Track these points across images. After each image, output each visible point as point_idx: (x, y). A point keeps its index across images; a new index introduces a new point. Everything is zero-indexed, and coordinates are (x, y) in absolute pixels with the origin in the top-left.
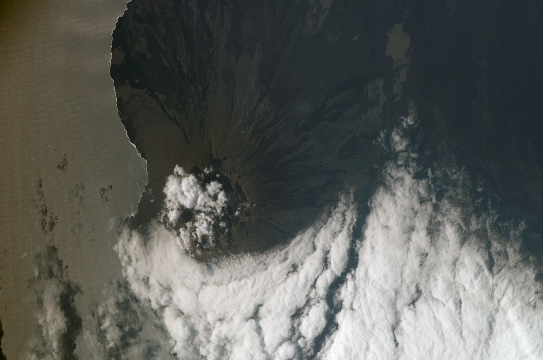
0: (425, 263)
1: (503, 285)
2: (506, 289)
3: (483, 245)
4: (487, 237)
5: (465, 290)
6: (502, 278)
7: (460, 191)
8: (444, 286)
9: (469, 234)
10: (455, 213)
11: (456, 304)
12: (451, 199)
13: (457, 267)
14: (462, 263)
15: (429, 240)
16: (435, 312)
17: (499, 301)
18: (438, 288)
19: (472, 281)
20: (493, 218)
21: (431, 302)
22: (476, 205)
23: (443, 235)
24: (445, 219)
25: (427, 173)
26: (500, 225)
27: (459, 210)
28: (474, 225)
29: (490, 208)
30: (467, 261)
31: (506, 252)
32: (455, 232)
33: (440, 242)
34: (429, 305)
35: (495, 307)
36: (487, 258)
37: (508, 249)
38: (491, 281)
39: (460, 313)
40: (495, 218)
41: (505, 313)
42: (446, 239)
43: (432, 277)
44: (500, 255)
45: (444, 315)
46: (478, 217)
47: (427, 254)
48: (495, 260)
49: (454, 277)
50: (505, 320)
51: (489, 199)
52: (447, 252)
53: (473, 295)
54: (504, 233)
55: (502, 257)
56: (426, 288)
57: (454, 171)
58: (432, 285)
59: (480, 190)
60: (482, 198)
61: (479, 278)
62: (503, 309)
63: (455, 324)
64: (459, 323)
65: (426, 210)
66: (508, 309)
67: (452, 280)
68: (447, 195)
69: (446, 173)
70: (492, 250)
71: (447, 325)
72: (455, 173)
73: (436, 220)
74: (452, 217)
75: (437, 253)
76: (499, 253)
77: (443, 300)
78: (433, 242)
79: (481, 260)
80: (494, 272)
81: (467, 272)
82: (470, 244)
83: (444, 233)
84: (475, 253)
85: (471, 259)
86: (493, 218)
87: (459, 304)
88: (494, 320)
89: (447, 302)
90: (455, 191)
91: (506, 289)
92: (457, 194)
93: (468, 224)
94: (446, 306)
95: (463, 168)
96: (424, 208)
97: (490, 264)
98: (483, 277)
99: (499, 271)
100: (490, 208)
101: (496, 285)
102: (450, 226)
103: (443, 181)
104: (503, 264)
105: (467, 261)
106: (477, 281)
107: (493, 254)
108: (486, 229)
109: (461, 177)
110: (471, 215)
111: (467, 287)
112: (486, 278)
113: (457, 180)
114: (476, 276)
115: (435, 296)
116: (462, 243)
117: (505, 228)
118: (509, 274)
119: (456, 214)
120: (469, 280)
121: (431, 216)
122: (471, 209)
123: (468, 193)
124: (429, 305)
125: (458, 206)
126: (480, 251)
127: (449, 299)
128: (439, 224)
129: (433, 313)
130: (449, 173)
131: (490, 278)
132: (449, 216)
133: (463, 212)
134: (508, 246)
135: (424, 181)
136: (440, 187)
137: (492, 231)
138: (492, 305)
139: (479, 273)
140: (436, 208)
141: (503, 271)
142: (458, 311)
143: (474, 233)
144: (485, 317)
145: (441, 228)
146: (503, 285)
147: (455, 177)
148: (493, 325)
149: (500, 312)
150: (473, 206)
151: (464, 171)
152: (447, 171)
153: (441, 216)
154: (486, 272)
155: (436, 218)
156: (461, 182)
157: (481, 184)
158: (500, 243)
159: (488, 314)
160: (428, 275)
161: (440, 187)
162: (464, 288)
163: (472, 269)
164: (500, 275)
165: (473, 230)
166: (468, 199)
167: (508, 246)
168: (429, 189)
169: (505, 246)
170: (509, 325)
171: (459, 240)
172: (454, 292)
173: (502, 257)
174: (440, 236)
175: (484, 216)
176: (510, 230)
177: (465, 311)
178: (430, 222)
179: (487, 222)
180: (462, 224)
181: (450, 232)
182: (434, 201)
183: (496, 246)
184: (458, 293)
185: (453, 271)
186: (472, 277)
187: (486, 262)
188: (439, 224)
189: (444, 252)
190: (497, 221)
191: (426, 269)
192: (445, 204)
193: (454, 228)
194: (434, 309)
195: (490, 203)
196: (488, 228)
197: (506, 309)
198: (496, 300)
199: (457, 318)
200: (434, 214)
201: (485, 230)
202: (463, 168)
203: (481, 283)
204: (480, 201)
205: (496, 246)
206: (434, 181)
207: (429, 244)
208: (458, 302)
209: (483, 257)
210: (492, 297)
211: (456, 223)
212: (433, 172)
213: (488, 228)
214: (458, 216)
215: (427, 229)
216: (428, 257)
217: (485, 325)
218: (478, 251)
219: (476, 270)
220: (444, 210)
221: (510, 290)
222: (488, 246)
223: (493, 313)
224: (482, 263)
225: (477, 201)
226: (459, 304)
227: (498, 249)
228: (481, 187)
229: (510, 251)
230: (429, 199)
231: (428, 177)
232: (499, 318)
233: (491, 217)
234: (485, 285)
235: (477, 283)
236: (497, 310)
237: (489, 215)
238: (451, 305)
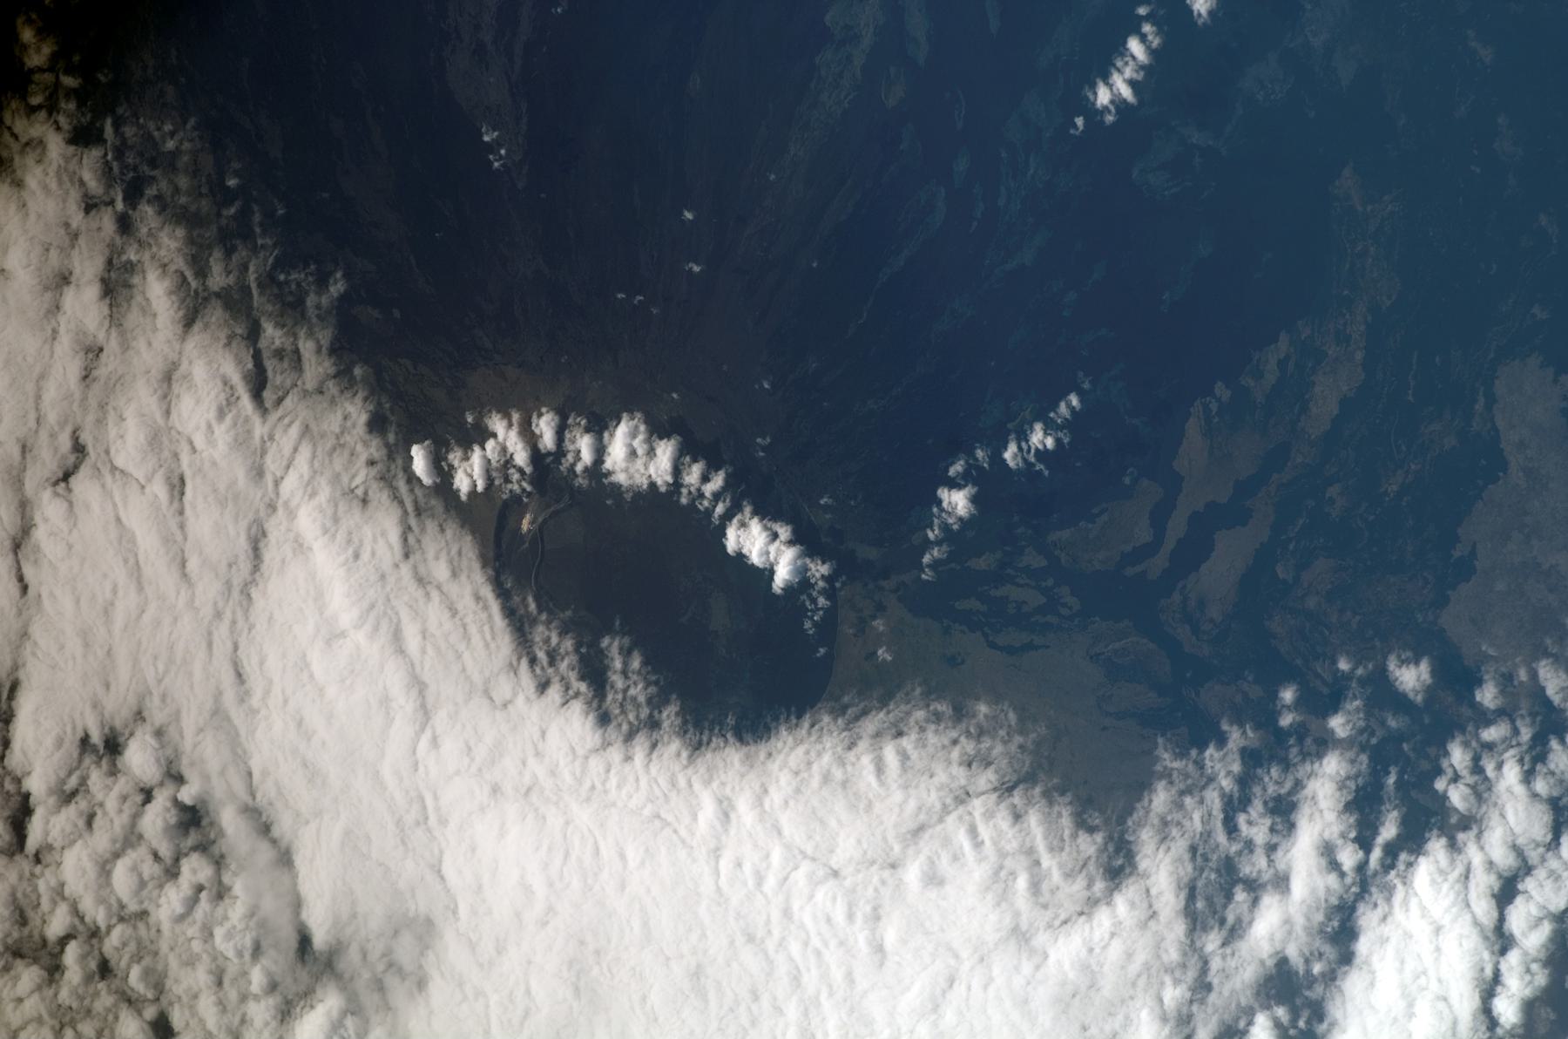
0: (95, 373)
1: (287, 439)
2: (296, 450)
3: (239, 331)
4: (250, 307)
5: (194, 450)
6: (286, 421)
7: (183, 182)
8: (142, 437)
9: (206, 299)
10: (170, 243)
11: (172, 487)
12: (161, 203)
13: (176, 387)
14: (187, 377)
15: (106, 311)
16: (120, 505)
17: (277, 483)
18: (127, 443)
19: (209, 426)
20: (266, 259)
21: (108, 478)
22: (224, 222)
23: (139, 298)
24: (147, 256)
25: (102, 130)
26: (282, 277)
27: (180, 232)
28: (218, 278)
29: (258, 230)
30: (199, 371)
31: (297, 351)
32: (171, 293)
33: (133, 318)
34: (103, 486)
35: (267, 500)
36: (250, 366)
37: (300, 345)
38: (259, 429)
39: (181, 512)
40: (271, 260)
41: (292, 515)
42: (147, 310)
43: (112, 412)
44: (281, 359)
45: (140, 513)
46: (229, 252)
47: (101, 350)
48: (270, 374)
49: (168, 413)
50: (292, 535)
51: (256, 208)
52: (150, 344)
53: (214, 463)
54: (290, 299)
55: (286, 364)
56: (96, 439)
57: (168, 127)
58: (113, 432)
59: (232, 182)
60: (237, 205)
61: (229, 419)
62: (286, 503)
63: (167, 540)
64: (179, 538)
65: (99, 229)
66: (299, 505)
67: (160, 421)
68: (151, 191)
69: (150, 137)
70: (262, 344)
71: (148, 542)
72: (172, 134)
73: (124, 258)
74: (163, 253)
75: (125, 347)
76: (279, 354)
77: (140, 474)
78: (116, 316)
79: (232, 368)
80: (268, 404)
81: (198, 402)
82: (206, 326)
83: (144, 293)
84: (220, 351)
85: (210, 367)
86: (266, 259)
87: (178, 486)
88: (264, 534)
89: (149, 480)
90: (171, 181)
91: (296, 450)
92: (177, 190)
93: (202, 273)
94: (147, 490)
95: (192, 122)
96: (94, 225)
97: (258, 383)
98: (237, 416)
99: (280, 401)
100: (258, 230)
101: (271, 438)
102: (158, 279)
103: (141, 154)
104: (288, 383)
105: (199, 371)
106: (224, 427)
107: (265, 354)
108: (249, 287)
109: (187, 146)
110: (210, 247)
111: (199, 441)
112: (247, 420)
113: (176, 154)
114: (221, 414)
115: (120, 461)
116: (189, 322)
117: (293, 287)
118: (304, 413)
119: (174, 245)
120: (203, 426)
121: (111, 245)
122: (211, 232)
123: (204, 190)
124: (103, 486)
125: (178, 223)
126: (234, 344)
127: (154, 472)
128: (130, 268)
129: (115, 505)
130: (156, 134)
131: (256, 420)
132: (154, 249)
133: (190, 241)
134: (302, 334)
135: (96, 153)
136: (135, 169)
137: (261, 294)
138: (259, 495)
139: (229, 404)
140: (125, 225)
141: (288, 402)
142: (176, 504)
143: (218, 295)
144: (244, 524)
145: (136, 280)
146: (287, 439)
147: (171, 145)
148: (261, 545)
149: (280, 511)
150: (213, 229)
151: (194, 128)
152: (152, 125)
153: (136, 246)
154: (246, 403)
155: (122, 252)
156: (186, 158)
157: (236, 165)
158: (283, 326)
159: (251, 516)
160: (102, 406)
161: (135, 169)
162: (191, 443)
163: (213, 394)
164: (280, 412)
165: (216, 289)
166: (205, 205)
167: (302, 334)
168: (107, 173)
169: (295, 336)
170: (300, 547)
171: (181, 313)
172: (166, 454)
173: (286, 364)
174: (134, 303)
175: (242, 253)
176: (307, 293)
177: (194, 507)
178: (110, 262)
179: (252, 269)
180: (189, 274)
181: (157, 292)
182: (120, 206)
183: (272, 334)
184: (176, 456)
185: (165, 397)
186: (212, 415)
187: (246, 378)
188: (130, 268)
189: (141, 344)
190: (274, 267)
191: (96, 388)
192: (147, 214)
193: (167, 283)
194: (117, 499)
195: (257, 218)
196: (254, 286)
197: (293, 503)
198: (269, 479)
199: (173, 524)
200: (118, 241)
201: (245, 290)
202: (192, 122)
203: (232, 433)
204: (233, 211)
205: (272, 334)
206: (120, 153)
207: (107, 323)
208: (176, 481)
209: (239, 362)
210: (259, 473)
211: (172, 268)
212: (117, 126)
213: (254, 286)
214: (179, 250)
215: (103, 280)
216: (103, 356)
217: (243, 543)
218: (228, 344)
219: (222, 396)
220: (144, 230)
221: (305, 452)
222: (254, 334)
223: (262, 514)
224: (236, 379)
225: (225, 212)
226: (178, 486)
227: (278, 342)
228: (236, 174)
229: (307, 347)
230: (107, 199)
231: (105, 141)
232: (276, 528)
233: (261, 255)
234: (241, 441)
235: (222, 433)
236: (272, 507)
237: (255, 250)
238: (159, 489)
